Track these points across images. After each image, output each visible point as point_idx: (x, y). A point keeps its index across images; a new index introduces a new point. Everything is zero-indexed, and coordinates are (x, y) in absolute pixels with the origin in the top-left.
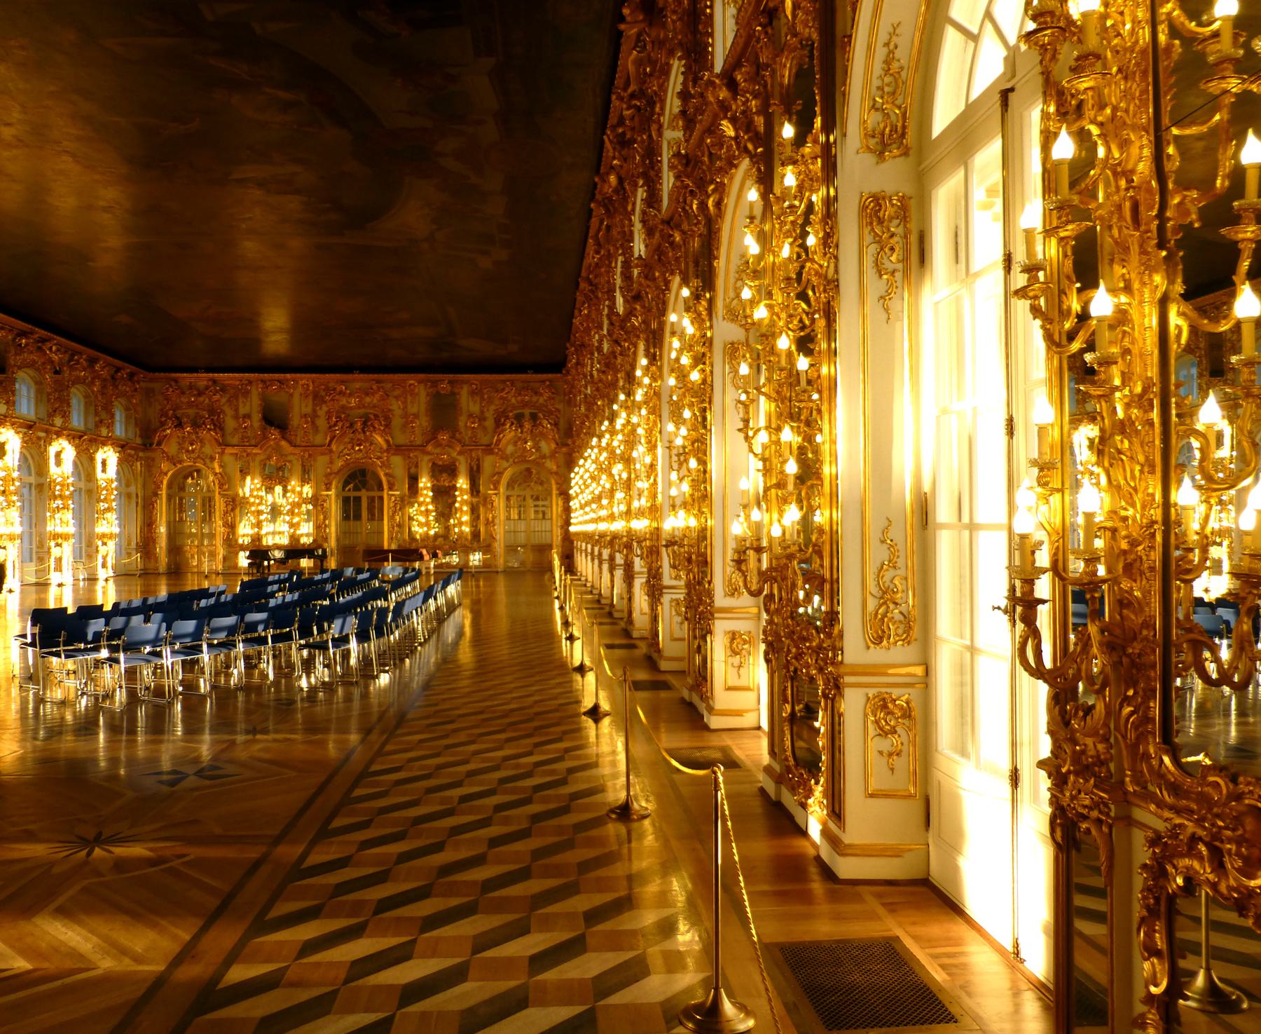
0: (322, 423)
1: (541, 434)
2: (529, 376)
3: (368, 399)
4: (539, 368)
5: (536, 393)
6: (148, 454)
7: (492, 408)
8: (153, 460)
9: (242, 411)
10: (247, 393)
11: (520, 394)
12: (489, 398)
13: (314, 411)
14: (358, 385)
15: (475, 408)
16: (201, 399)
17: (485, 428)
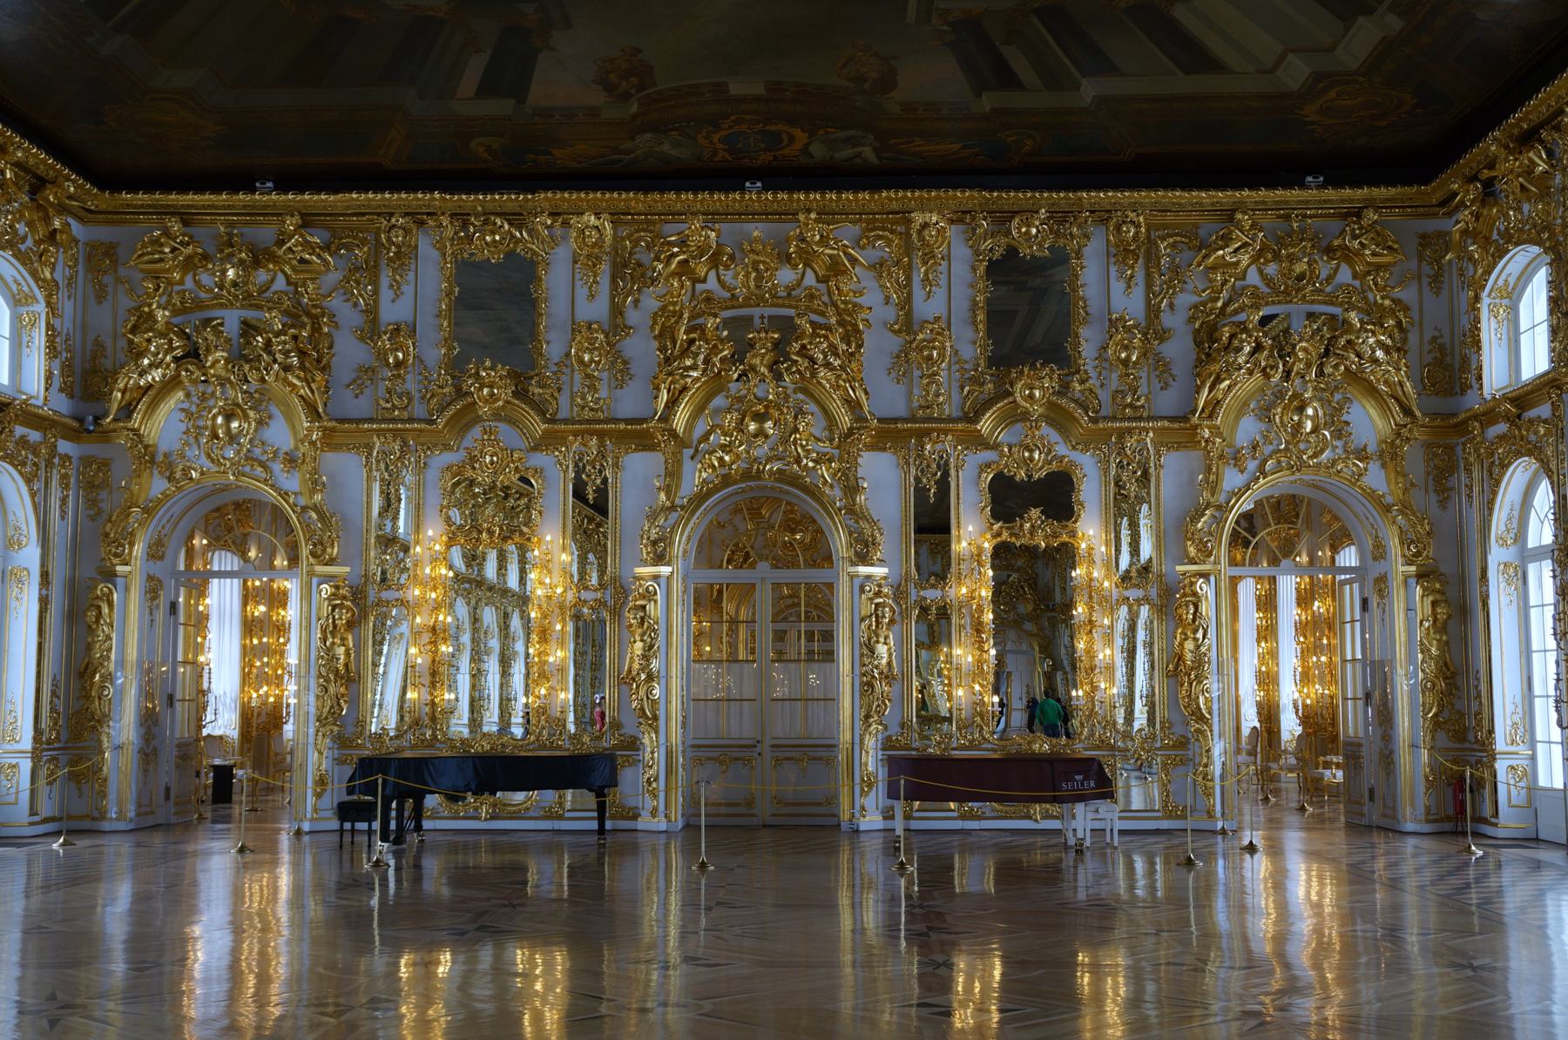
0: (641, 348)
1: (1354, 377)
2: (1311, 195)
3: (786, 276)
4: (1342, 167)
5: (1329, 251)
6: (93, 449)
7: (1185, 299)
8: (105, 465)
9: (392, 311)
10: (404, 257)
11: (1277, 257)
12: (1175, 270)
13: (617, 311)
14: (756, 230)
15: (1129, 302)
16: (262, 276)
17: (1162, 368)
